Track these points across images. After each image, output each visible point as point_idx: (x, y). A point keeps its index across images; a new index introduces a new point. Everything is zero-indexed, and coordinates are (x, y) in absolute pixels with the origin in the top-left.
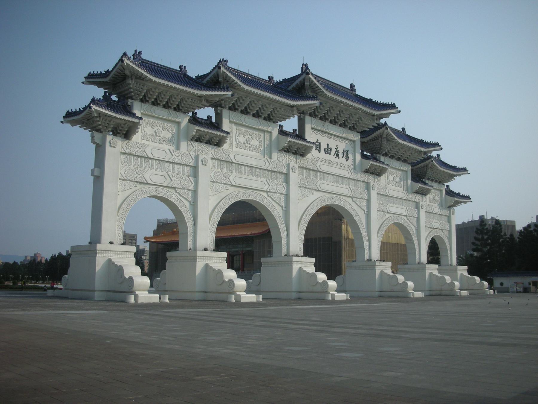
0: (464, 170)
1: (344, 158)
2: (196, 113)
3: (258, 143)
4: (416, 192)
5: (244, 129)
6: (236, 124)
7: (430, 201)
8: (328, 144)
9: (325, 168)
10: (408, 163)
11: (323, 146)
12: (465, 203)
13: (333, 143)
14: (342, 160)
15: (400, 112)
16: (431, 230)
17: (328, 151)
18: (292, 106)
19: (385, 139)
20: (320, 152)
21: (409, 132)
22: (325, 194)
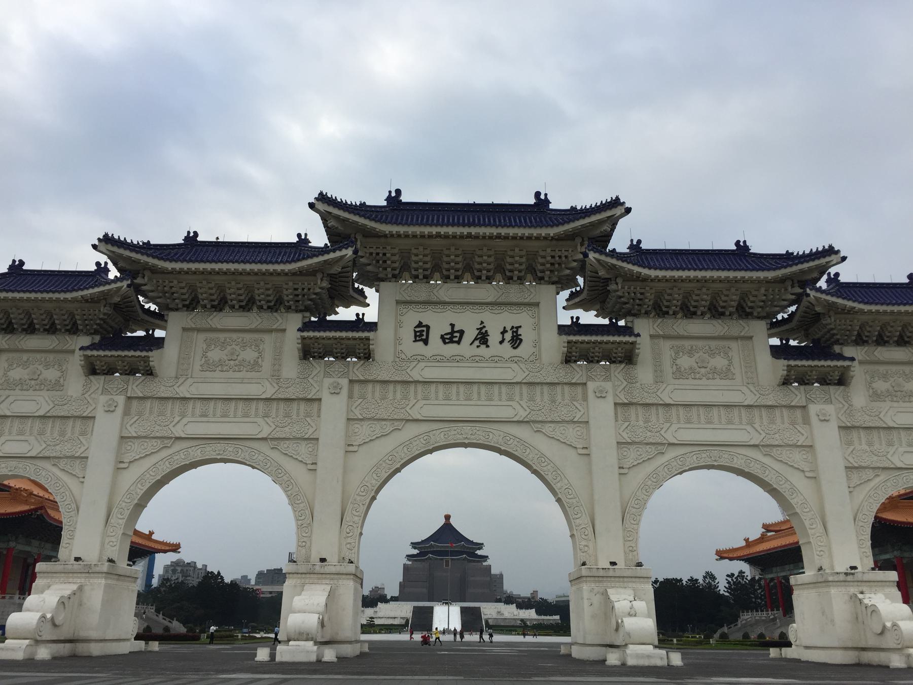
1: (507, 345)
2: (121, 331)
3: (256, 355)
4: (784, 384)
5: (222, 336)
6: (199, 330)
7: (876, 396)
8: (453, 326)
9: (432, 373)
10: (759, 318)
13: (468, 323)
15: (628, 210)
17: (453, 337)
19: (619, 280)
20: (426, 342)
21: (756, 248)
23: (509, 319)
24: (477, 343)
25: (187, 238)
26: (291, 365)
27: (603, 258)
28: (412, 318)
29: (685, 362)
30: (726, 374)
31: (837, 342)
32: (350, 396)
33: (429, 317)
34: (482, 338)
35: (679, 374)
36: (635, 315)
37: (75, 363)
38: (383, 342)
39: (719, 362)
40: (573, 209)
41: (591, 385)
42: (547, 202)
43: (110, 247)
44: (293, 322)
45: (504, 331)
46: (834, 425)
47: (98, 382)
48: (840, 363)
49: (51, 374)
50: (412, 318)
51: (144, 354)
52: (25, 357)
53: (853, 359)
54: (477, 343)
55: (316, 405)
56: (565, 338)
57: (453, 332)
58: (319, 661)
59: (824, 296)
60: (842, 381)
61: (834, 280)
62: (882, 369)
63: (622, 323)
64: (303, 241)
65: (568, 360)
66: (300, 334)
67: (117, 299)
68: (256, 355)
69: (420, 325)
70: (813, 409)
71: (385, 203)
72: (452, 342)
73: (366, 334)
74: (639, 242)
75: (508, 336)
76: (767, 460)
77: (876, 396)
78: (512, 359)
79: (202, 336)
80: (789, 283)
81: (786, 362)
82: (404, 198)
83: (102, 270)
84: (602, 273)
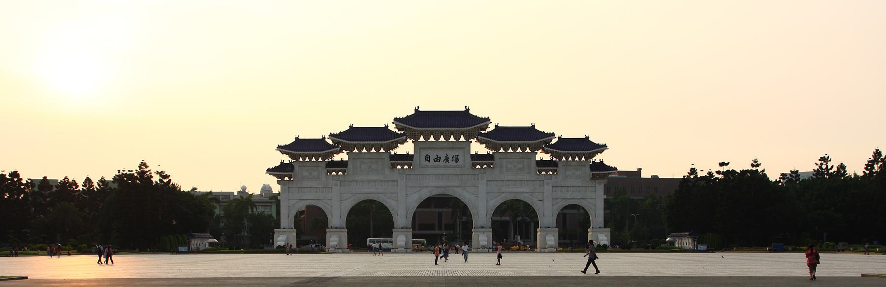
0: (605, 146)
17: (437, 159)
23: (454, 153)
26: (387, 171)
28: (424, 153)
29: (509, 166)
33: (430, 153)
34: (447, 159)
42: (468, 110)
46: (550, 187)
49: (315, 174)
50: (424, 153)
63: (491, 153)
79: (358, 161)
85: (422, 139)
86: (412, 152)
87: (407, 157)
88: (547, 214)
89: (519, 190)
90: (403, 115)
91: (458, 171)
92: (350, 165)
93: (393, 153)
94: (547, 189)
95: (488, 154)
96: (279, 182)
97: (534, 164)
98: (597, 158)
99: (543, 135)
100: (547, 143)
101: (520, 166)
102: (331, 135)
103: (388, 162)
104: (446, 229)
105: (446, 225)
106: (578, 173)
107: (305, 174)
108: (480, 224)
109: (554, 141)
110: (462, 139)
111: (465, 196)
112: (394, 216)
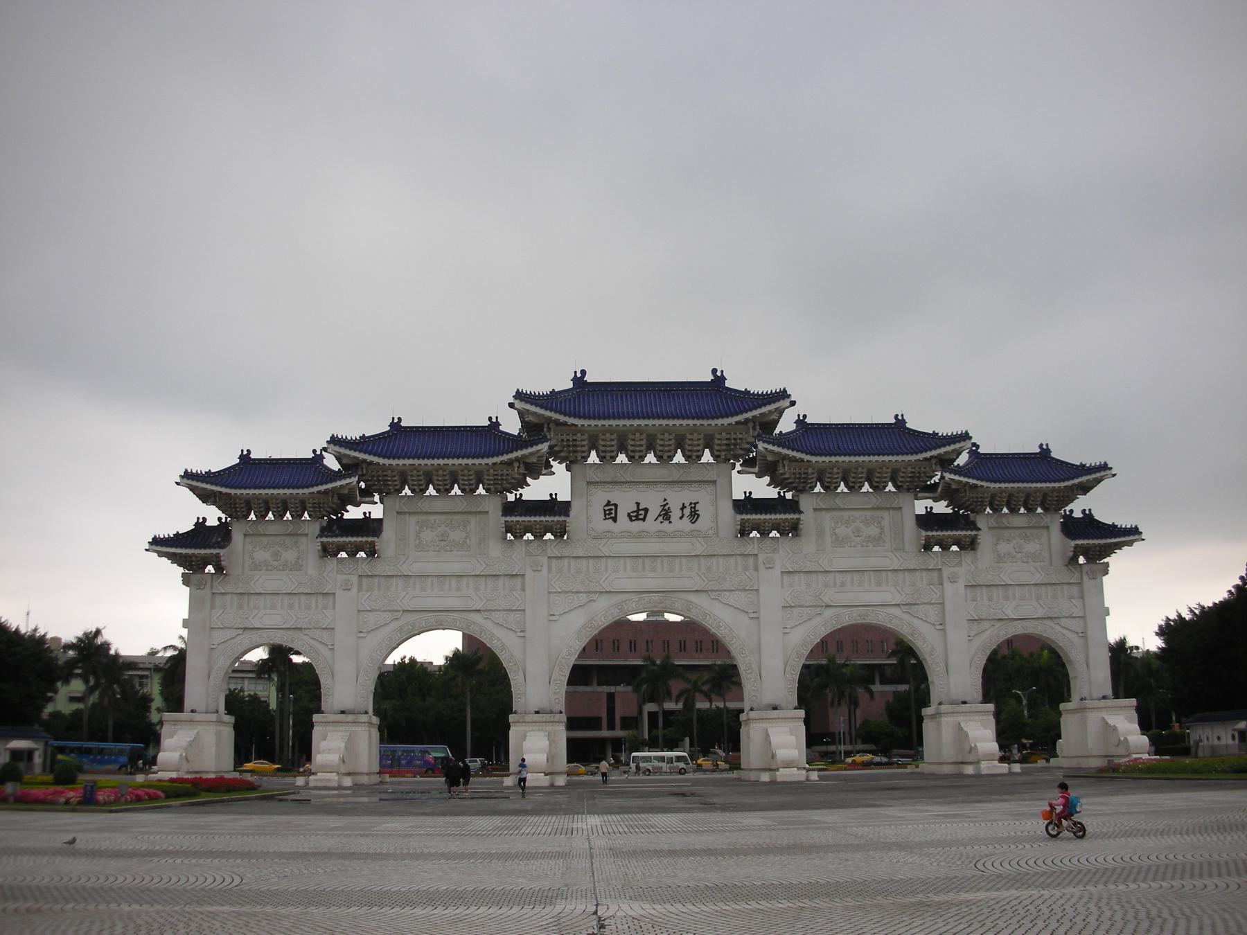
0: (1104, 467)
3: (464, 535)
5: (432, 518)
7: (1000, 558)
8: (638, 504)
10: (908, 490)
11: (626, 507)
12: (1130, 544)
13: (652, 500)
14: (680, 524)
15: (793, 403)
16: (1000, 623)
17: (639, 514)
18: (510, 463)
20: (615, 519)
22: (627, 596)
24: (661, 519)
25: (392, 425)
27: (770, 447)
29: (842, 531)
30: (877, 540)
31: (973, 511)
32: (550, 571)
33: (616, 495)
34: (666, 515)
35: (839, 542)
36: (802, 491)
37: (311, 546)
38: (575, 521)
39: (873, 531)
40: (747, 392)
41: (761, 558)
42: (723, 379)
43: (337, 448)
44: (493, 506)
45: (684, 507)
46: (961, 585)
47: (331, 563)
48: (969, 533)
49: (289, 555)
50: (600, 497)
51: (370, 539)
52: (265, 540)
53: (979, 529)
54: (661, 519)
55: (518, 581)
56: (739, 517)
57: (638, 510)
58: (552, 785)
59: (957, 478)
60: (970, 545)
61: (974, 453)
62: (1007, 533)
63: (789, 496)
64: (494, 425)
65: (744, 532)
66: (503, 519)
67: (346, 492)
68: (464, 535)
69: (608, 504)
70: (946, 573)
71: (570, 385)
72: (638, 519)
73: (562, 518)
74: (805, 416)
75: (687, 511)
76: (906, 616)
77: (1000, 558)
78: (690, 535)
79: (412, 520)
80: (934, 461)
81: (924, 533)
82: (588, 379)
83: (318, 458)
84: (770, 458)
85: (593, 458)
86: (564, 495)
87: (553, 506)
88: (956, 669)
89: (874, 598)
90: (541, 386)
91: (700, 548)
92: (388, 532)
93: (511, 498)
94: (954, 592)
95: (781, 498)
96: (186, 581)
97: (910, 525)
98: (1077, 507)
99: (934, 440)
100: (945, 463)
101: (873, 531)
102: (334, 440)
103: (497, 519)
104: (623, 727)
105: (623, 719)
106: (1031, 547)
107: (262, 555)
108: (768, 697)
109: (963, 459)
110: (707, 457)
111: (723, 618)
112: (515, 678)
